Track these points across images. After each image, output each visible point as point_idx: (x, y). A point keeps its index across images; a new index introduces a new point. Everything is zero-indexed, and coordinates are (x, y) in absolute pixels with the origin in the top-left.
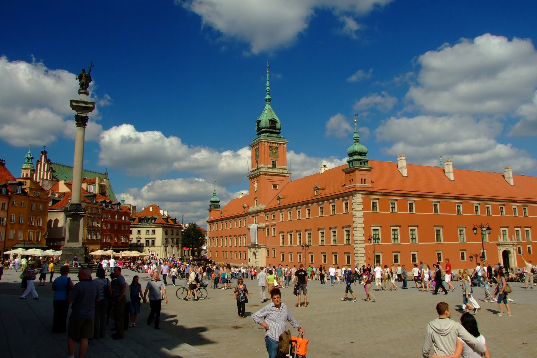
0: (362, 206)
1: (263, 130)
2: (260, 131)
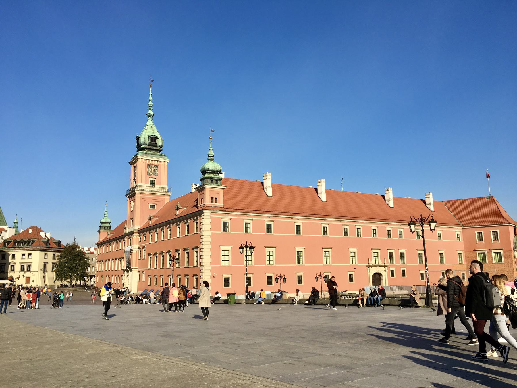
0: (210, 227)
1: (142, 147)
2: (139, 148)
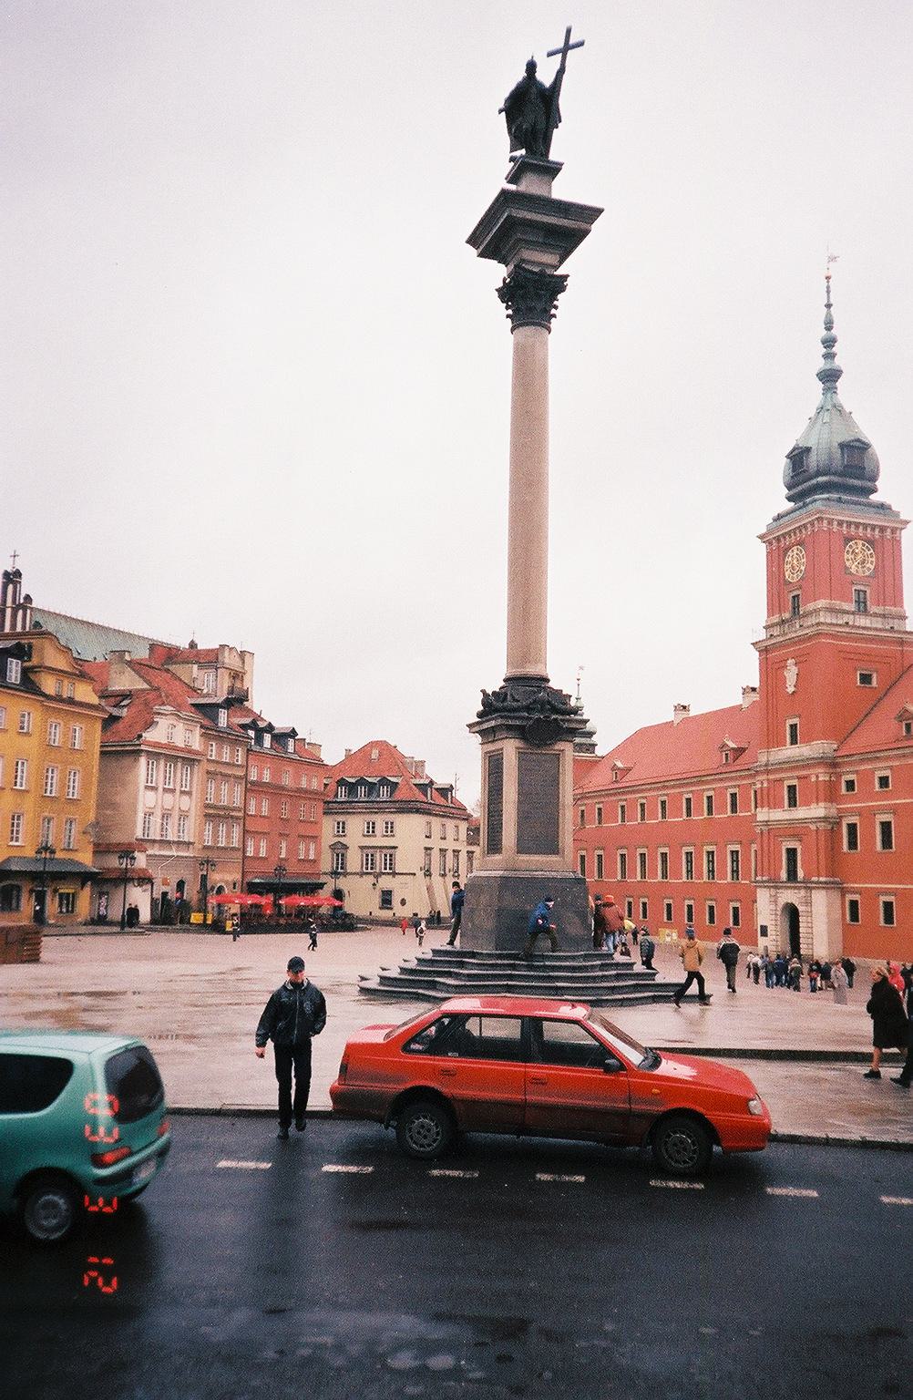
1: (821, 479)
